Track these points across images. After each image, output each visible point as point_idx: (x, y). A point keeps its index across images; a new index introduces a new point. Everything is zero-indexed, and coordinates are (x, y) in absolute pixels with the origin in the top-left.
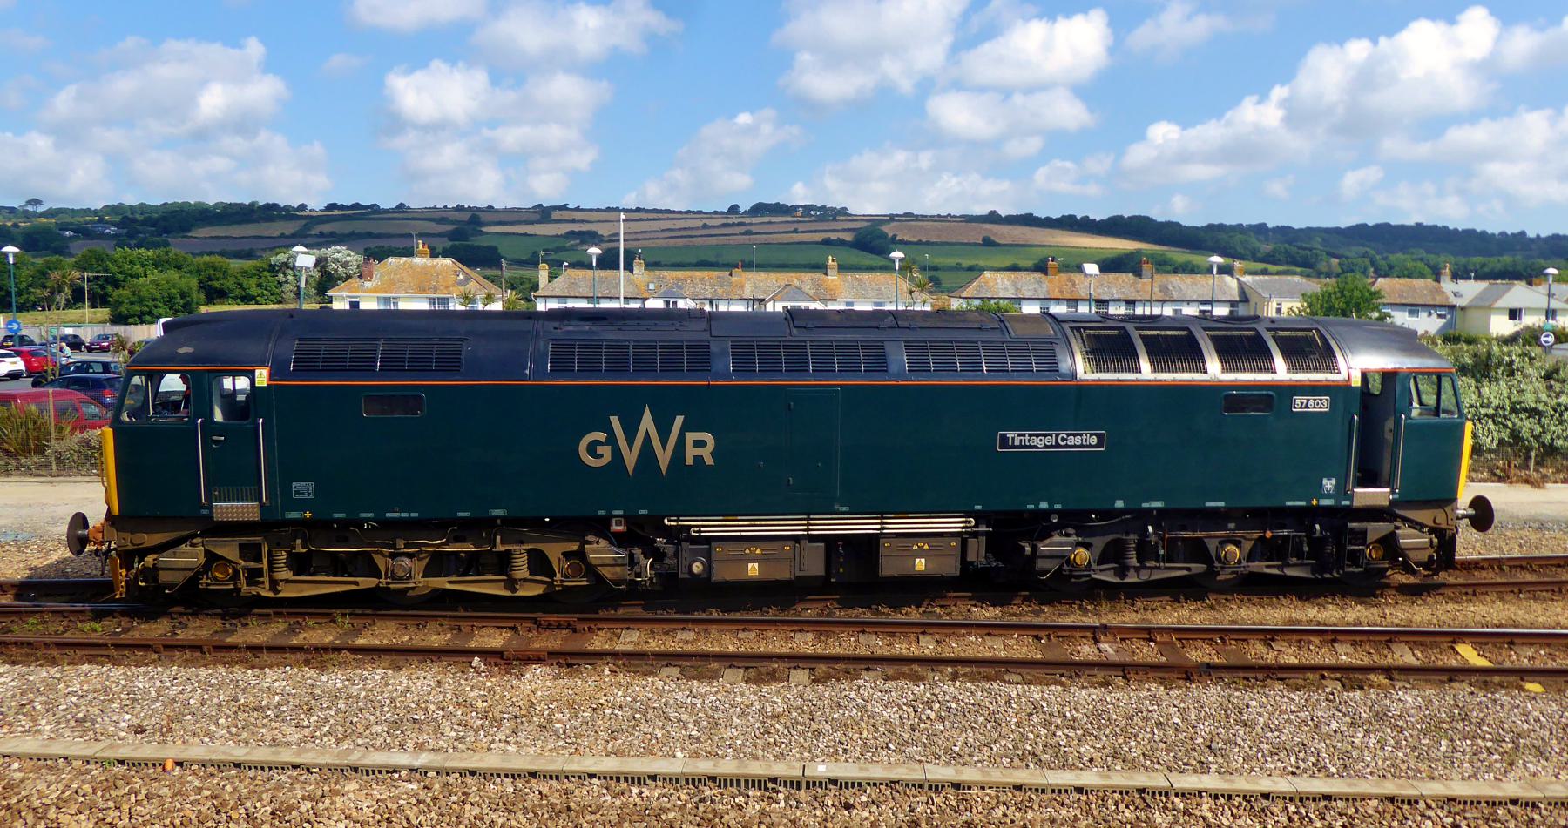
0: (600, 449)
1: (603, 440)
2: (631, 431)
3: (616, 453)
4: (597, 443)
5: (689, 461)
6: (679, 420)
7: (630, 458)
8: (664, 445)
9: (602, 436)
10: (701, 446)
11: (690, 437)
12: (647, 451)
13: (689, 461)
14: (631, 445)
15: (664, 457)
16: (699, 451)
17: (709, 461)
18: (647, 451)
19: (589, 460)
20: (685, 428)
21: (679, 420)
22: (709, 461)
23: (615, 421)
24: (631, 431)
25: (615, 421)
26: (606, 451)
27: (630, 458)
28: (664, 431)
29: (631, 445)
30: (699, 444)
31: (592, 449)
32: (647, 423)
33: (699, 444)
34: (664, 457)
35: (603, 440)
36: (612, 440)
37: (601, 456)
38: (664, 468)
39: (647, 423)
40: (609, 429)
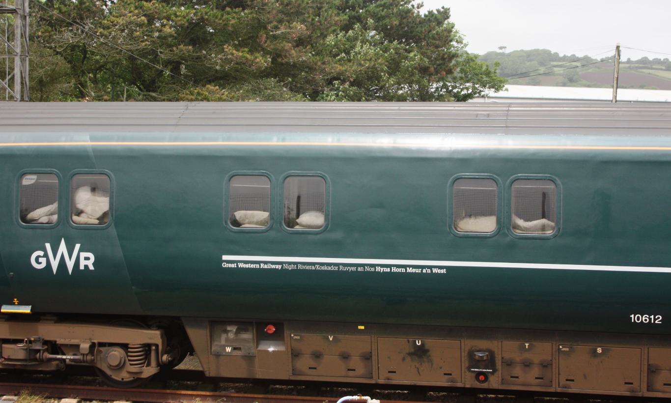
0: (41, 260)
1: (42, 255)
5: (82, 267)
6: (78, 246)
7: (55, 265)
8: (70, 257)
9: (41, 253)
10: (88, 261)
11: (83, 255)
12: (62, 264)
13: (82, 267)
14: (55, 256)
15: (70, 265)
17: (91, 268)
18: (62, 264)
20: (81, 250)
21: (78, 246)
22: (91, 268)
23: (48, 246)
25: (48, 246)
26: (43, 261)
27: (55, 265)
29: (55, 256)
30: (87, 259)
32: (63, 248)
33: (87, 259)
34: (70, 265)
35: (42, 255)
36: (46, 255)
37: (40, 263)
38: (70, 272)
39: (63, 248)
40: (45, 250)
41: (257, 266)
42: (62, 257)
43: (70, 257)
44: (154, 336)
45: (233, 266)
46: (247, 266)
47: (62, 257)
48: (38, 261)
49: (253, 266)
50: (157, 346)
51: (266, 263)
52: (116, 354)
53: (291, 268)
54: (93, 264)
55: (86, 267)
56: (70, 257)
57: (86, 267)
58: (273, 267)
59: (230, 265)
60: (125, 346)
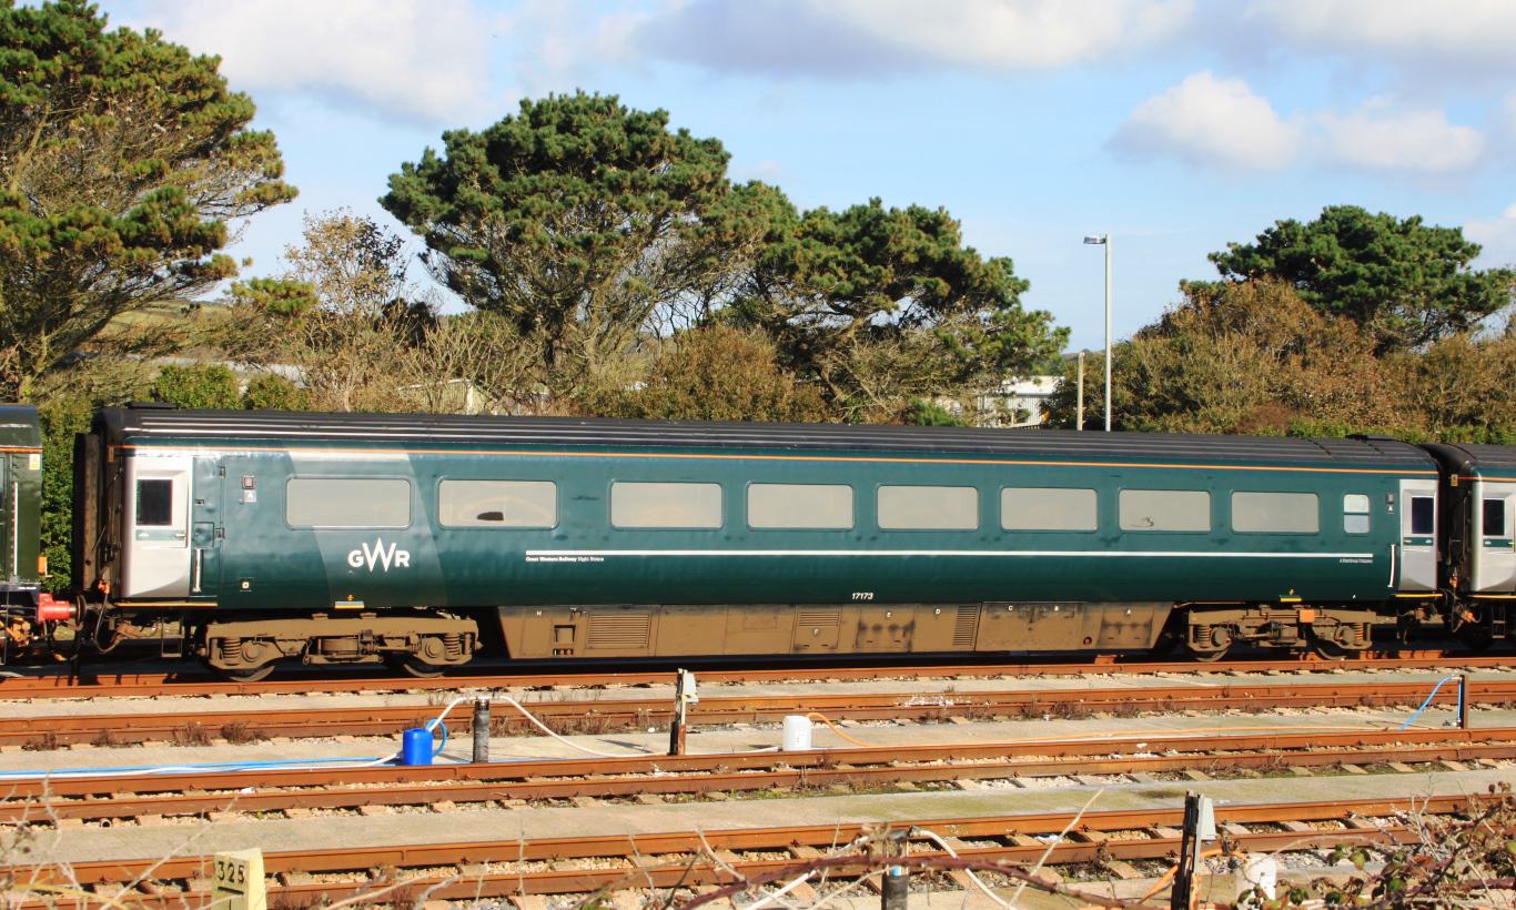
0: (358, 559)
2: (372, 550)
5: (398, 565)
6: (394, 546)
8: (387, 555)
9: (359, 552)
11: (399, 553)
12: (379, 563)
13: (398, 565)
16: (402, 560)
17: (406, 565)
18: (379, 563)
19: (354, 565)
20: (397, 548)
21: (394, 546)
22: (406, 565)
23: (365, 546)
24: (372, 550)
25: (365, 546)
28: (387, 550)
30: (402, 556)
32: (379, 547)
33: (402, 556)
36: (363, 554)
39: (379, 547)
40: (362, 549)
44: (471, 625)
50: (473, 634)
52: (436, 645)
53: (584, 560)
54: (409, 562)
55: (401, 564)
56: (387, 555)
57: (401, 564)
59: (533, 559)
60: (442, 637)
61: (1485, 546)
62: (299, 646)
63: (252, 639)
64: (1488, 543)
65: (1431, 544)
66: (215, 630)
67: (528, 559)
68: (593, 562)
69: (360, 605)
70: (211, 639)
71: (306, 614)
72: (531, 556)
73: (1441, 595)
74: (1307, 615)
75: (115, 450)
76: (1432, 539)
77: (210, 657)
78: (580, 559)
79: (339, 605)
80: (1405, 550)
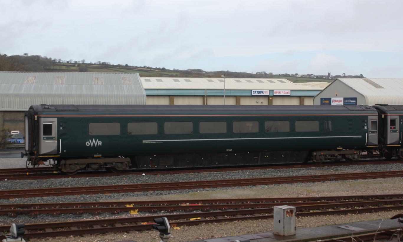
0: (88, 144)
2: (92, 142)
3: (90, 144)
4: (87, 144)
5: (99, 145)
6: (97, 140)
7: (92, 145)
8: (96, 143)
9: (88, 142)
10: (100, 143)
11: (99, 142)
13: (99, 145)
15: (96, 144)
17: (101, 145)
20: (98, 141)
21: (97, 140)
22: (101, 145)
23: (90, 140)
24: (92, 142)
25: (90, 140)
26: (89, 144)
28: (96, 141)
30: (100, 143)
31: (87, 144)
32: (94, 141)
33: (100, 143)
34: (96, 144)
36: (90, 143)
39: (94, 141)
40: (89, 141)
41: (150, 143)
42: (94, 143)
43: (96, 143)
45: (145, 143)
46: (148, 143)
47: (94, 143)
48: (88, 144)
49: (149, 143)
51: (152, 142)
54: (102, 144)
55: (100, 145)
56: (96, 143)
57: (100, 145)
58: (154, 143)
59: (144, 143)
61: (391, 132)
62: (84, 166)
63: (72, 164)
64: (391, 131)
65: (377, 133)
66: (63, 162)
67: (143, 143)
68: (147, 143)
69: (100, 156)
70: (62, 164)
71: (86, 158)
72: (144, 142)
73: (378, 146)
74: (344, 152)
75: (37, 117)
76: (376, 131)
77: (62, 169)
78: (157, 142)
79: (95, 156)
80: (370, 135)
